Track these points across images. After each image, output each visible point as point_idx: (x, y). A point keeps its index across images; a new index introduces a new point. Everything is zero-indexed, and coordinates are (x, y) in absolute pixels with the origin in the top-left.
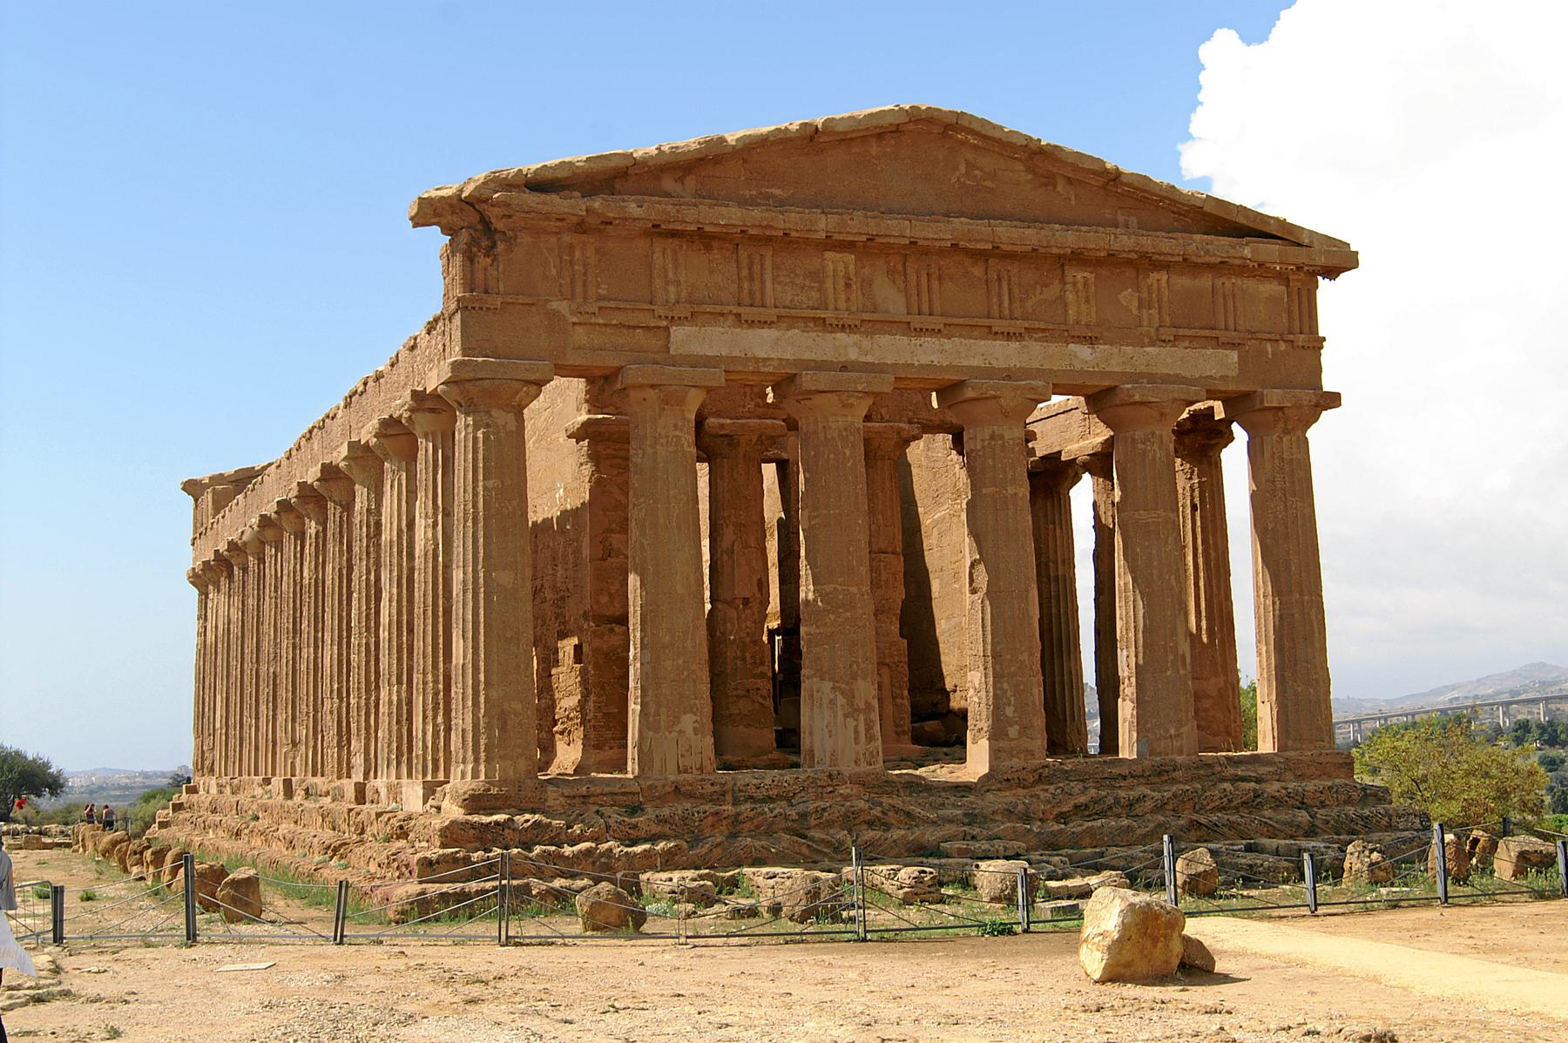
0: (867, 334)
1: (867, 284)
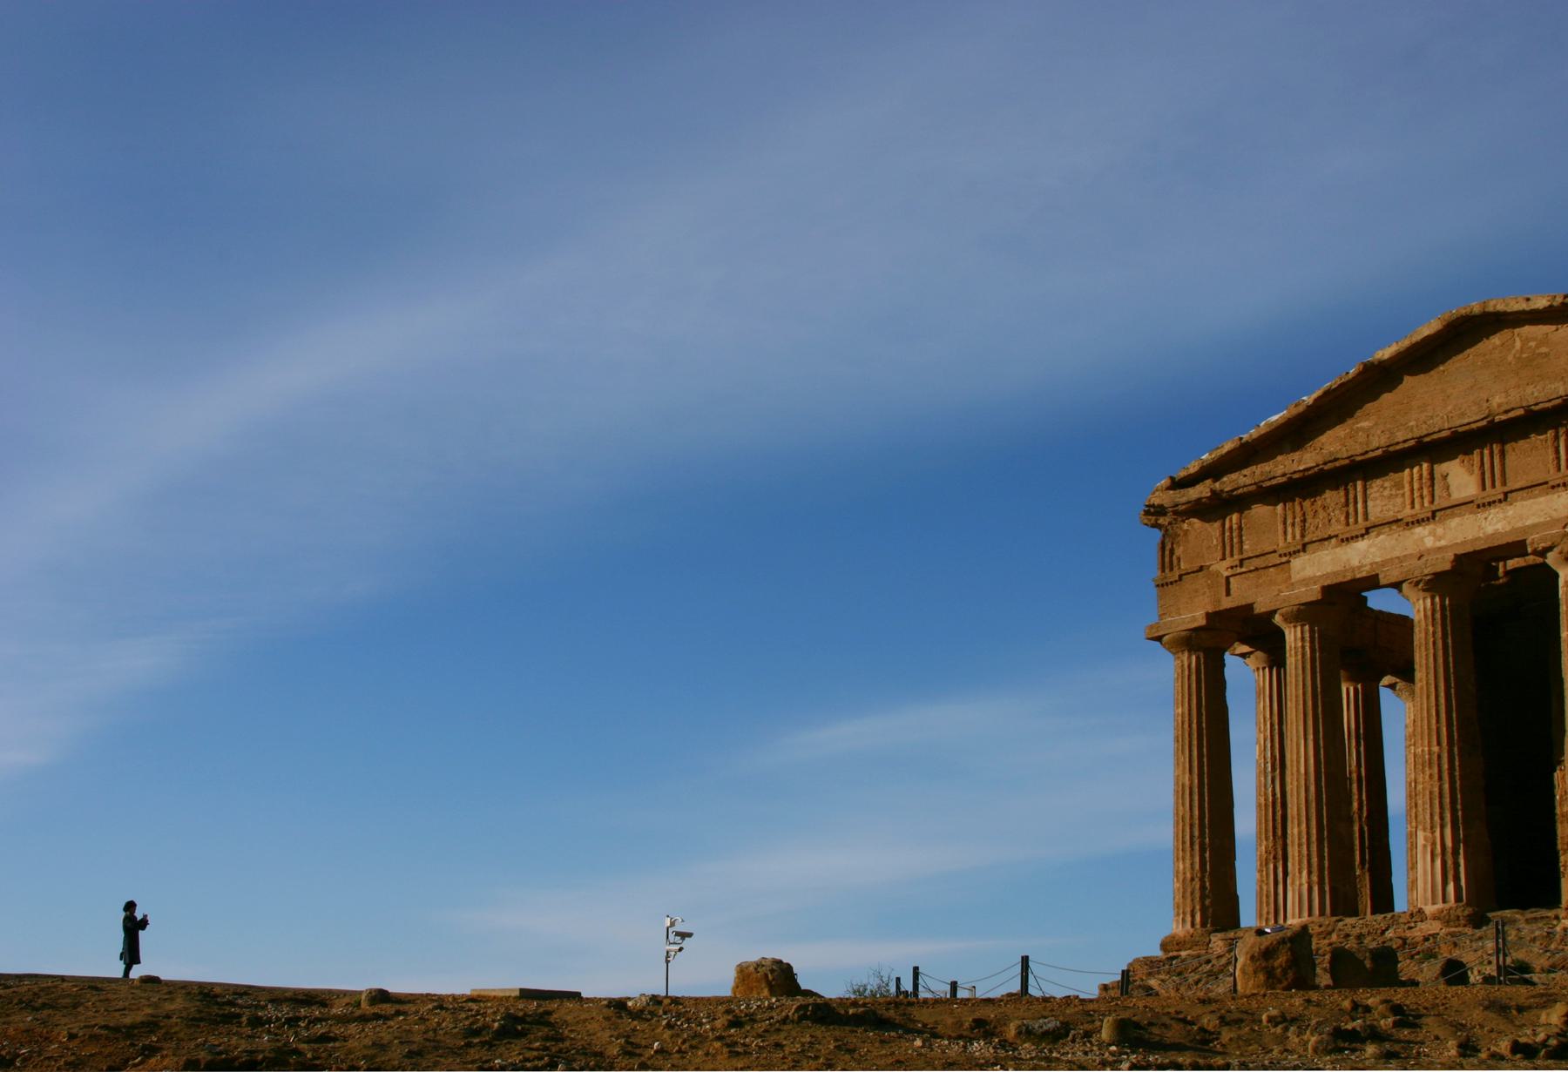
0: (1440, 521)
1: (1445, 477)
